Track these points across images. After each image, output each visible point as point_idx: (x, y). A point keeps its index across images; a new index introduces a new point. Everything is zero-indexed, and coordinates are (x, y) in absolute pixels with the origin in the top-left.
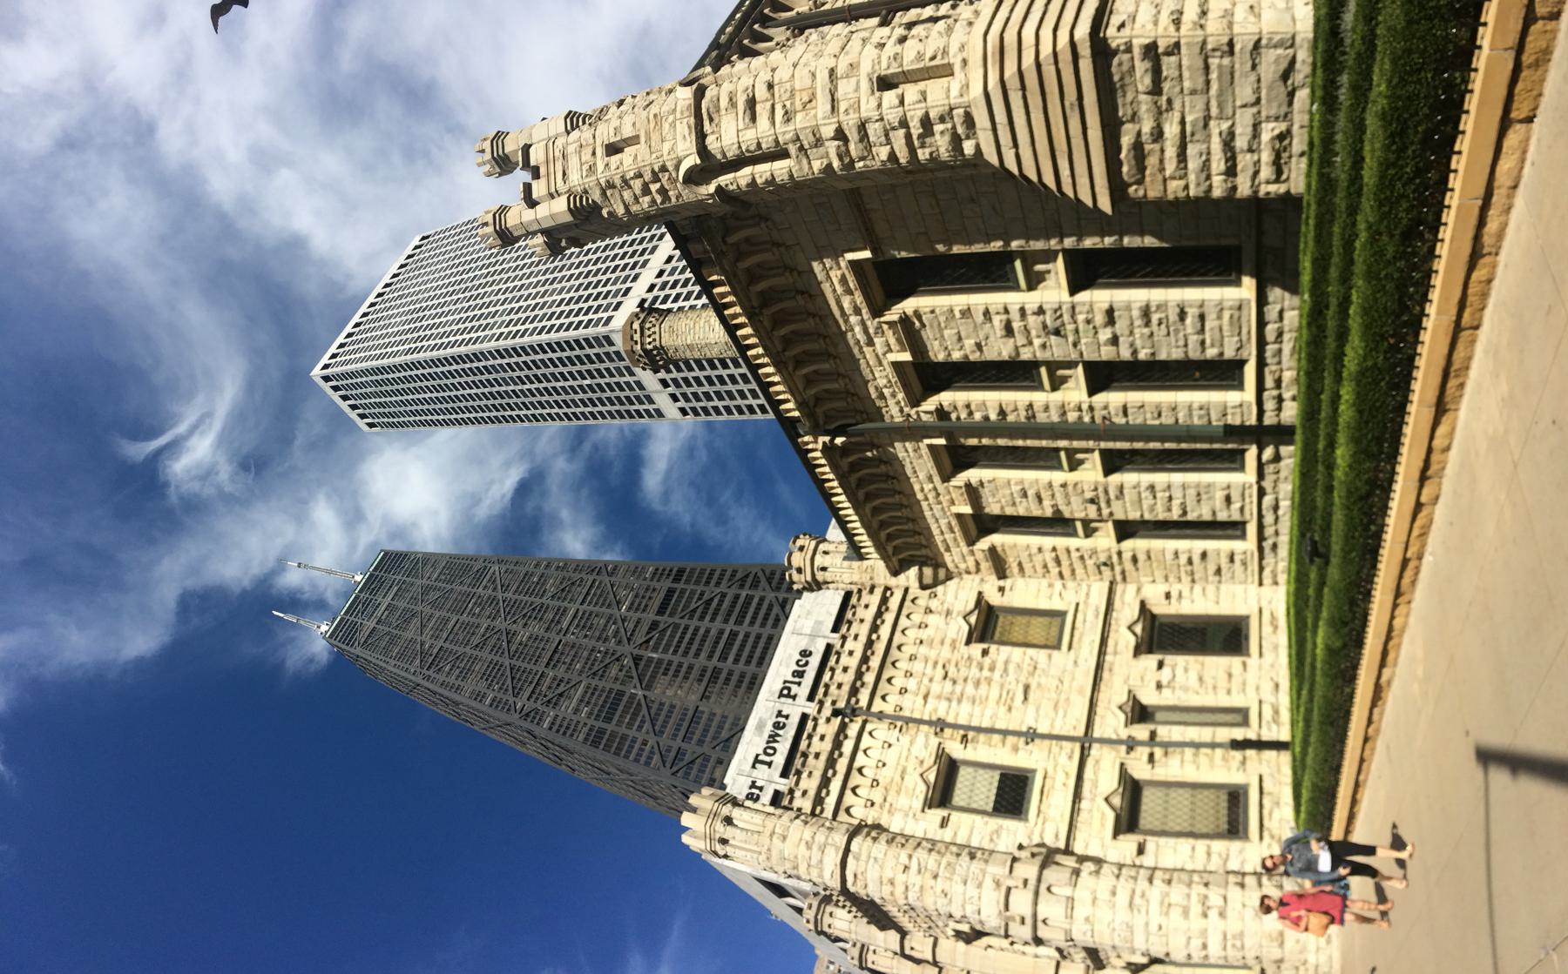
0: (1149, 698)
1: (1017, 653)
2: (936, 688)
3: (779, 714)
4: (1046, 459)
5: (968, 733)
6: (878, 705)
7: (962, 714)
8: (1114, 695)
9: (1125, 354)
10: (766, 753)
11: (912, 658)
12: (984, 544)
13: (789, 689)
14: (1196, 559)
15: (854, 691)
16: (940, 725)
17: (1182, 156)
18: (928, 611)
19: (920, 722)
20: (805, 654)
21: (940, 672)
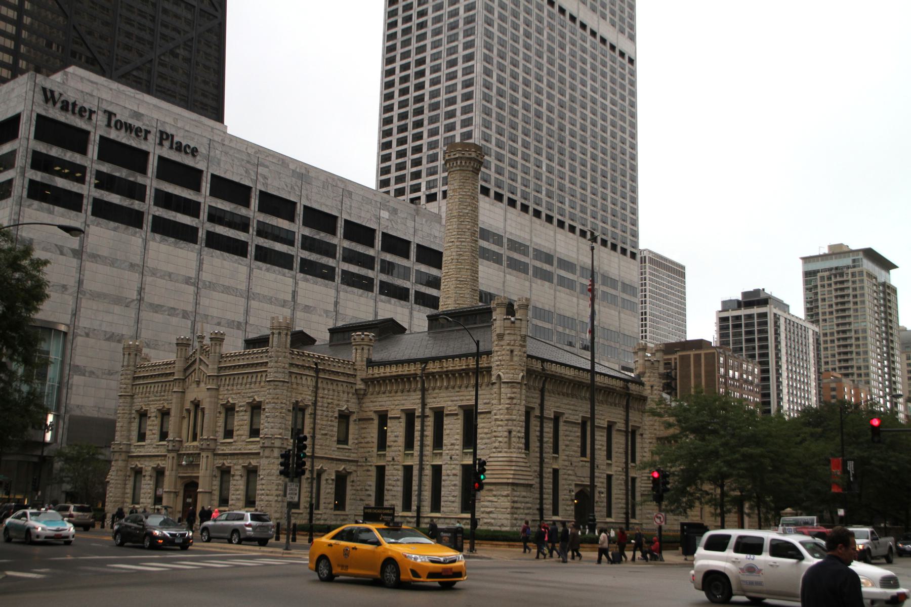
0: (324, 477)
1: (336, 429)
2: (325, 400)
3: (147, 132)
4: (409, 445)
5: (314, 414)
6: (320, 381)
7: (319, 412)
8: (326, 466)
9: (443, 478)
10: (117, 122)
11: (334, 390)
12: (375, 417)
13: (167, 138)
14: (368, 493)
15: (323, 370)
16: (315, 404)
17: (489, 501)
18: (348, 393)
19: (316, 397)
20: (194, 152)
21: (330, 401)
